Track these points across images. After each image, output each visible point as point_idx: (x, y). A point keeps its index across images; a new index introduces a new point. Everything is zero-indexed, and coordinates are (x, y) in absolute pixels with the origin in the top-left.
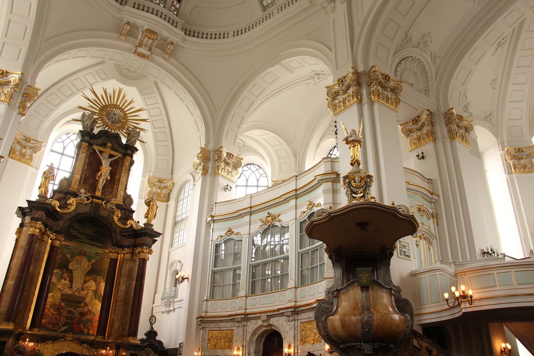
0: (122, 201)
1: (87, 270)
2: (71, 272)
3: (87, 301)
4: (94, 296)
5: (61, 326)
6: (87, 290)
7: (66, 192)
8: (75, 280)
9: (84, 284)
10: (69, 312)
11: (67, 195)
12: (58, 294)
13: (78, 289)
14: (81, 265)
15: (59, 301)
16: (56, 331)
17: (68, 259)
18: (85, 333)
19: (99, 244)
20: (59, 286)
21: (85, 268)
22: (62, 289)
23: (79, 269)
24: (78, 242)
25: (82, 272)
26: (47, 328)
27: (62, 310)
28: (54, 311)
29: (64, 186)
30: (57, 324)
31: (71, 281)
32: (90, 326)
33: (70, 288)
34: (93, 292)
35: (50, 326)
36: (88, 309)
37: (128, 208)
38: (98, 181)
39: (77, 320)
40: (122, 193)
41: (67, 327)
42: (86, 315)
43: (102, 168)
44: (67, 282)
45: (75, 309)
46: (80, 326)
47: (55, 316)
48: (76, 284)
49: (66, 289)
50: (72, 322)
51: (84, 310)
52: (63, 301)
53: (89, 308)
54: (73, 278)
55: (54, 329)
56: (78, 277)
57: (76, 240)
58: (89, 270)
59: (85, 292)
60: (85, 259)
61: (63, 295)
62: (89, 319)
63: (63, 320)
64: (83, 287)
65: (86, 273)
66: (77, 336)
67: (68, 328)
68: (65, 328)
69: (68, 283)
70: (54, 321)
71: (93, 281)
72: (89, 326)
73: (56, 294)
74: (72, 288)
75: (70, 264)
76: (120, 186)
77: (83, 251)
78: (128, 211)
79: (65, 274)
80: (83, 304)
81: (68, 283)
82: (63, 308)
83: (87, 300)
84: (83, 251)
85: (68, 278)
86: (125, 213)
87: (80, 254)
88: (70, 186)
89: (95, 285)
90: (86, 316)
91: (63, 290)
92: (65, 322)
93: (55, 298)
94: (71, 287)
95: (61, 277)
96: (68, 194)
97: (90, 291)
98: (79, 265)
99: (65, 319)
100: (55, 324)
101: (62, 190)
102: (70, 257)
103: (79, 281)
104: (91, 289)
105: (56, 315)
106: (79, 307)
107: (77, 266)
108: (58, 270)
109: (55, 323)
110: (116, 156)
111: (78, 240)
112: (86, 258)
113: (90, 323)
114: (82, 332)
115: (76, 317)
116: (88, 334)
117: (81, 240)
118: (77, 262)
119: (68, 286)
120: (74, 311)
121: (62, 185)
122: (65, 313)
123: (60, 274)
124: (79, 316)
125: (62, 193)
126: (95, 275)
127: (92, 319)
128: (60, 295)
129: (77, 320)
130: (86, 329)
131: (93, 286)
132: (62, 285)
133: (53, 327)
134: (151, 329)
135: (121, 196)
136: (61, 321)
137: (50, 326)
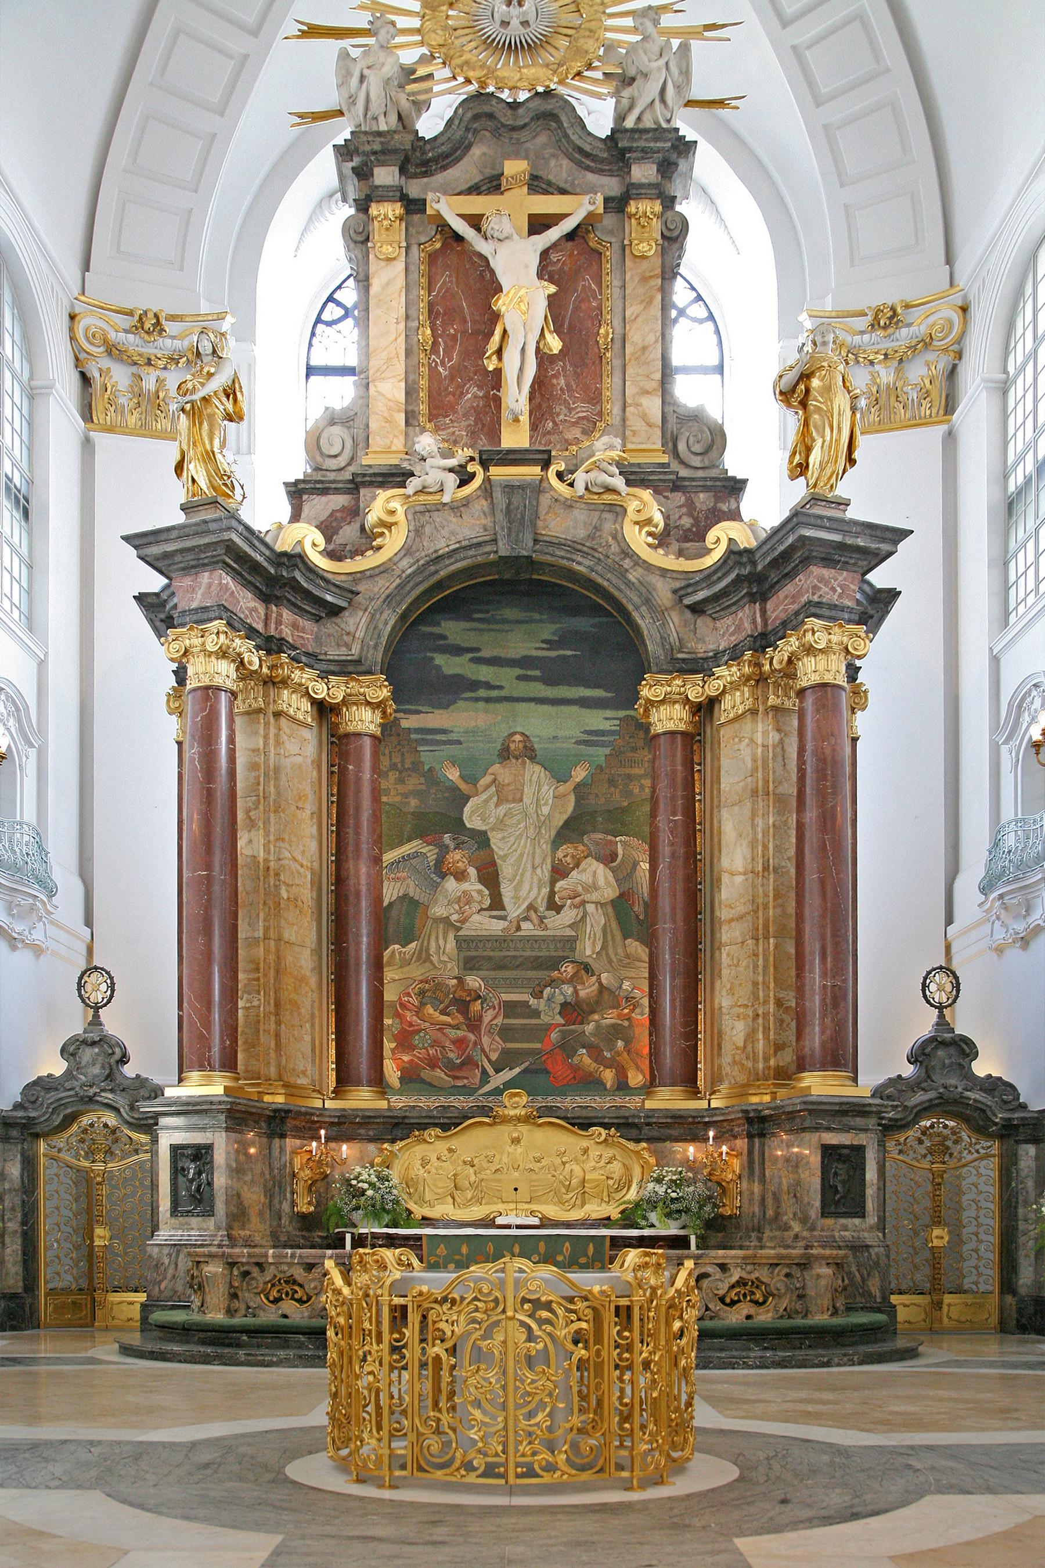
0: (658, 446)
1: (559, 820)
2: (482, 839)
3: (588, 952)
4: (614, 925)
5: (490, 1070)
6: (576, 907)
7: (352, 481)
8: (506, 870)
9: (553, 883)
10: (511, 1009)
11: (363, 491)
12: (441, 942)
13: (531, 907)
14: (521, 800)
15: (454, 968)
16: (467, 1091)
17: (455, 789)
18: (608, 1086)
19: (587, 692)
20: (438, 910)
21: (545, 810)
22: (454, 917)
23: (514, 821)
24: (481, 705)
25: (531, 832)
26: (430, 1085)
27: (477, 1006)
28: (443, 1012)
29: (336, 456)
30: (469, 1062)
31: (490, 877)
32: (625, 1054)
33: (491, 908)
34: (610, 910)
35: (438, 1073)
36: (601, 984)
37: (700, 474)
38: (498, 372)
39: (554, 1036)
40: (653, 406)
41: (517, 1070)
42: (593, 1012)
43: (501, 304)
44: (473, 886)
45: (538, 995)
46: (576, 1060)
47: (453, 1033)
48: (517, 889)
49: (476, 918)
50: (538, 1046)
51: (582, 993)
52: (471, 969)
53: (604, 981)
54: (494, 864)
55: (460, 1083)
56: (522, 855)
57: (473, 695)
58: (565, 817)
59: (568, 915)
60: (534, 772)
61: (463, 943)
62: (614, 1026)
63: (492, 1045)
64: (552, 894)
65: (553, 833)
66: (569, 1103)
67: (523, 1072)
68: (507, 1075)
69: (479, 892)
70: (451, 1055)
71: (598, 859)
72: (619, 1054)
73: (433, 944)
74: (503, 909)
75: (467, 810)
76: (630, 371)
77: (518, 738)
78: (706, 489)
79: (456, 858)
80: (568, 969)
81: (479, 892)
82: (479, 997)
83: (588, 949)
84: (518, 738)
85: (472, 872)
86: (690, 504)
87: (505, 754)
88: (368, 447)
89: (611, 879)
90: (596, 1017)
91: (464, 921)
92: (505, 1052)
93: (435, 959)
94: (497, 903)
95: (441, 870)
96: (364, 484)
97: (590, 908)
98: (514, 801)
99: (497, 1038)
100: (463, 1064)
101: (332, 476)
102: (461, 777)
103: (528, 874)
104: (595, 896)
105: (457, 1027)
106: (552, 983)
107: (502, 810)
108: (416, 843)
109: (458, 1061)
110: (563, 216)
111: (482, 693)
112: (537, 768)
113: (620, 1044)
114: (591, 1083)
115: (549, 1028)
116: (622, 1086)
117: (495, 693)
118: (497, 791)
119: (480, 902)
120: (532, 1001)
121: (322, 454)
122: (495, 1017)
123: (432, 857)
124: (560, 1020)
125: (337, 491)
126: (600, 836)
127: (626, 1023)
128: (451, 944)
129: (554, 1036)
130: (606, 1067)
131: (601, 882)
132: (450, 903)
133: (455, 1078)
134: (936, 1031)
135: (650, 425)
136: (483, 1050)
137: (438, 1073)
